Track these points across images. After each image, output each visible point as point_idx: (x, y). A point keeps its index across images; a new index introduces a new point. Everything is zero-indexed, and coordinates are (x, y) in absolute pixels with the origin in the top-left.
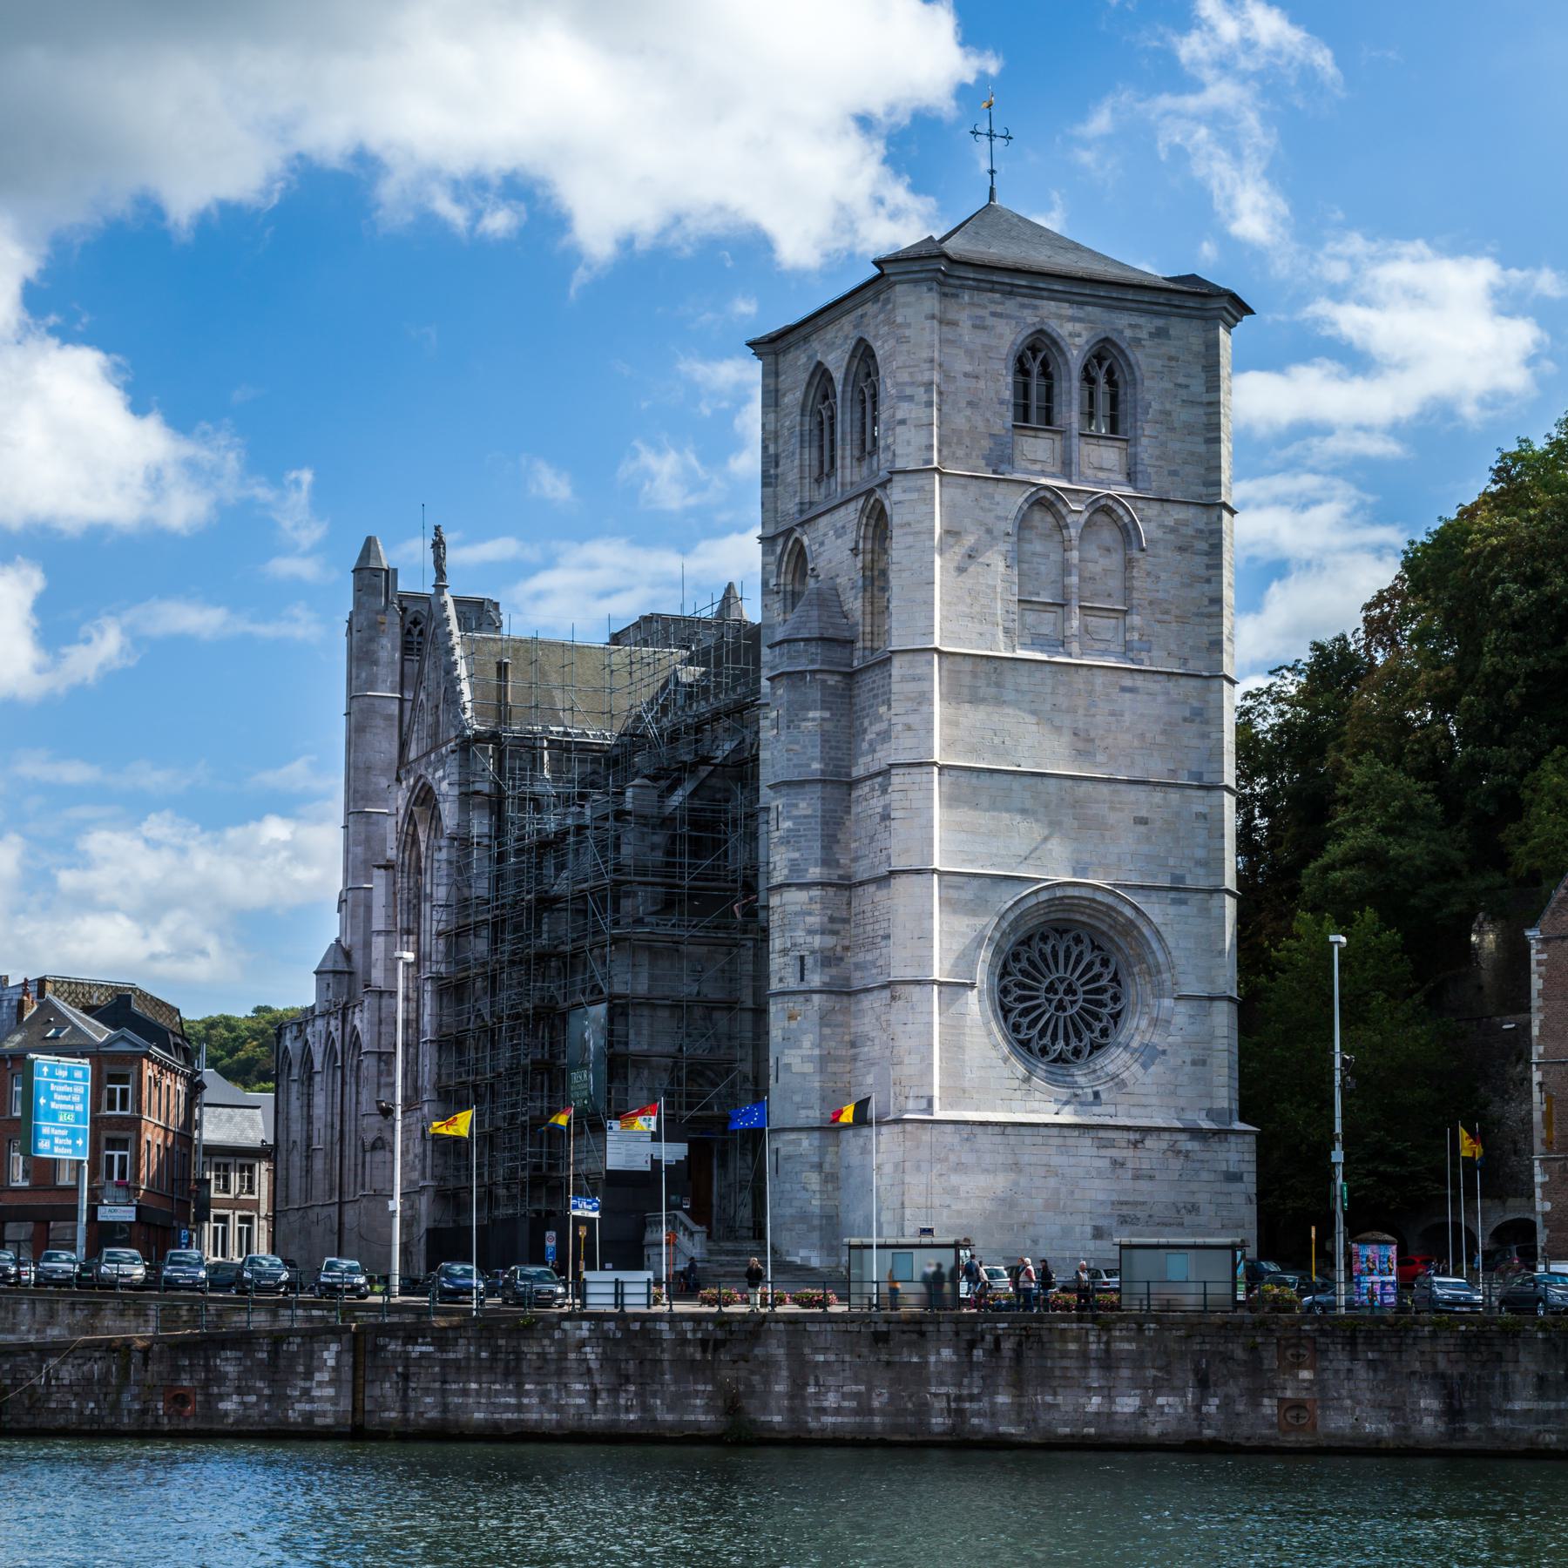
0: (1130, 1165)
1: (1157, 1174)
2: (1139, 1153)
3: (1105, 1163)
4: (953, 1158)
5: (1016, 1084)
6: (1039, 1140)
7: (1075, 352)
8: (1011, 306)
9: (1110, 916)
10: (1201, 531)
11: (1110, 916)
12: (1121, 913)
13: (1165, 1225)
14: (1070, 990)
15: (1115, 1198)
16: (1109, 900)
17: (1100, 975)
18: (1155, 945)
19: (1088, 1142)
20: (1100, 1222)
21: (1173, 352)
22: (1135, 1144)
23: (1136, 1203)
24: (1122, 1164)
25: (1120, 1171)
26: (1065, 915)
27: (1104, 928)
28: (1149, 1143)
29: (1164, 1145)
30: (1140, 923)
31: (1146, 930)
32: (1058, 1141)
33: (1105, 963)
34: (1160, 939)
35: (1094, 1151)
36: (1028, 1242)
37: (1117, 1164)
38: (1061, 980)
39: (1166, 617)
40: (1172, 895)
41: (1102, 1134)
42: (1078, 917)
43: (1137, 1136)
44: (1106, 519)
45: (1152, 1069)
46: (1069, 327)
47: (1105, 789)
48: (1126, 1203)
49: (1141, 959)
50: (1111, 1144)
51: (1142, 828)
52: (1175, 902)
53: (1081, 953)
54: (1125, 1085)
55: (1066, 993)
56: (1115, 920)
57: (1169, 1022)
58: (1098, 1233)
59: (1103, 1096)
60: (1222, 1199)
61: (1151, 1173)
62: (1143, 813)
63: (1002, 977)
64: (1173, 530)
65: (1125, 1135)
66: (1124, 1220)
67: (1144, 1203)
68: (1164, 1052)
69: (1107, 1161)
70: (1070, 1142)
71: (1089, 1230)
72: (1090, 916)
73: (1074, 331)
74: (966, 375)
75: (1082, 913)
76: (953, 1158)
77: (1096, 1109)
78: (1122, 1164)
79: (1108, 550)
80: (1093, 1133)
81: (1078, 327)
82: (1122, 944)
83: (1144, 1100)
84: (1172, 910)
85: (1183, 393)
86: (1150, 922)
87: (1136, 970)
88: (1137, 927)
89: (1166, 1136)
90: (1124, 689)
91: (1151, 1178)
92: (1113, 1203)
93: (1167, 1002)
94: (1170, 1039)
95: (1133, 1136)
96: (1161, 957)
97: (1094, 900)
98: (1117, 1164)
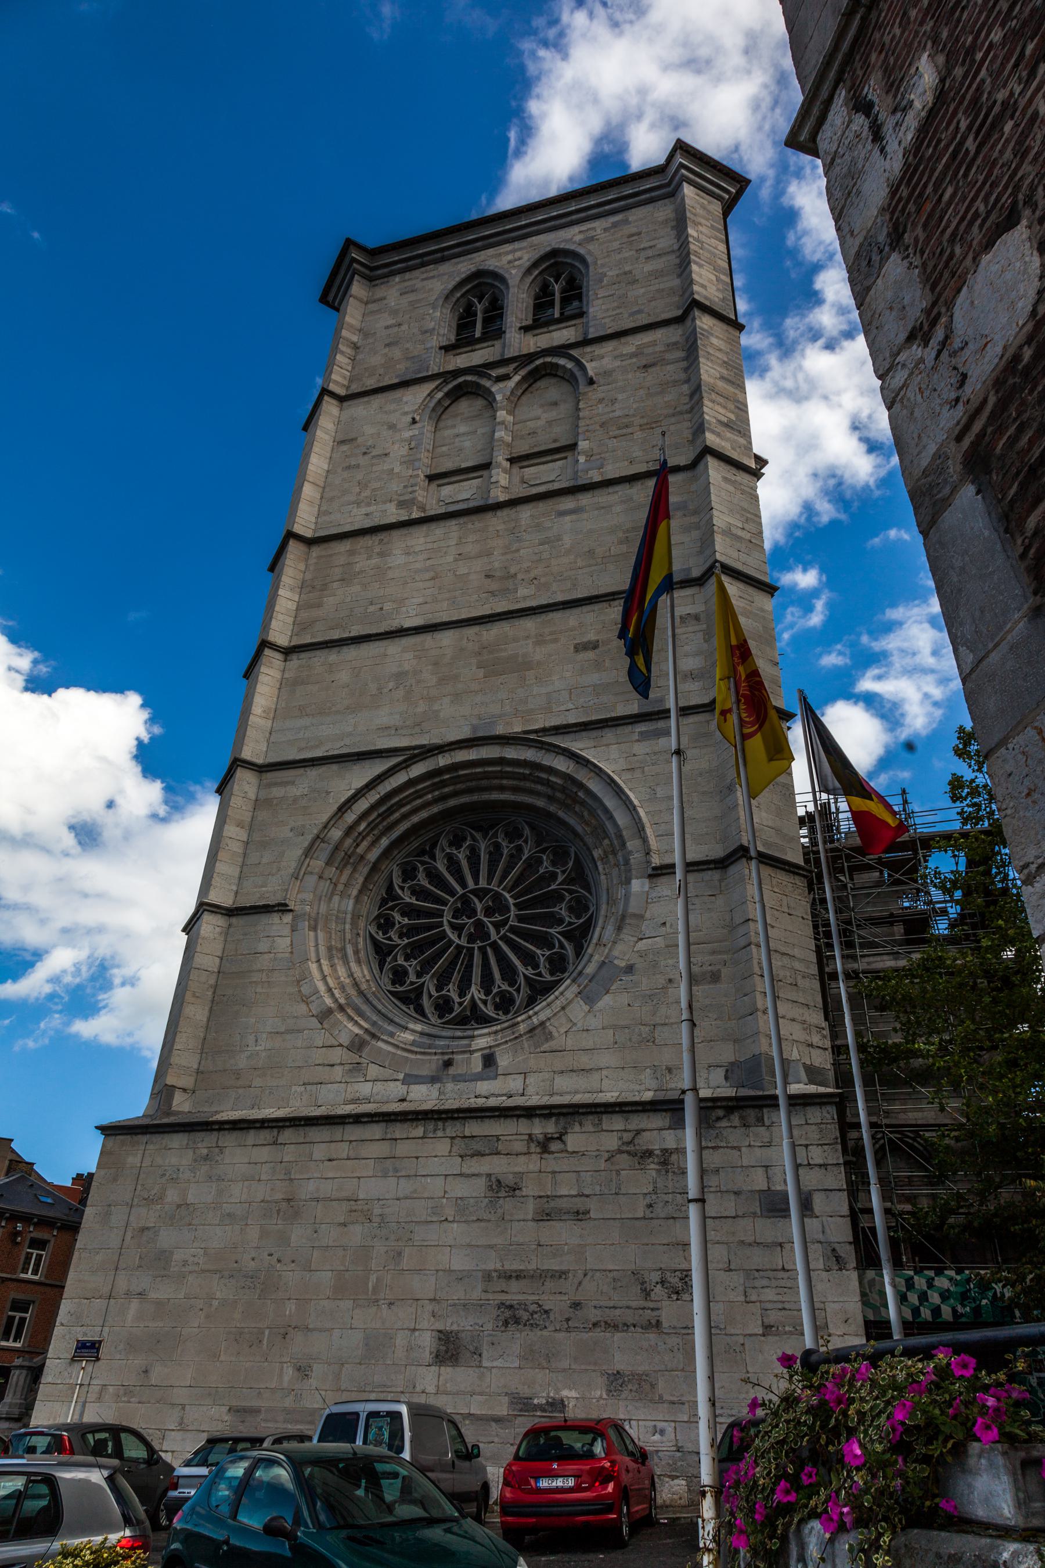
0: (530, 1189)
1: (592, 1205)
2: (552, 1163)
3: (475, 1189)
4: (172, 1196)
5: (337, 1055)
6: (343, 1150)
7: (513, 272)
8: (445, 268)
9: (540, 781)
10: (675, 343)
11: (540, 781)
12: (551, 770)
13: (613, 1326)
14: (498, 906)
15: (492, 1264)
16: (529, 754)
17: (553, 876)
18: (610, 802)
19: (442, 1147)
20: (449, 1324)
21: (634, 230)
22: (544, 1145)
23: (542, 1276)
24: (514, 1189)
25: (507, 1205)
26: (475, 797)
27: (540, 803)
28: (574, 1140)
29: (611, 1142)
30: (582, 775)
31: (594, 785)
32: (381, 1149)
33: (560, 855)
34: (618, 792)
35: (455, 1165)
36: (289, 1372)
37: (503, 1189)
38: (480, 893)
39: (629, 430)
40: (642, 727)
41: (473, 1128)
42: (495, 796)
43: (550, 1127)
44: (553, 380)
45: (606, 1001)
46: (510, 257)
47: (529, 624)
48: (519, 1276)
49: (600, 832)
50: (493, 1148)
51: (590, 655)
52: (644, 736)
53: (519, 849)
54: (549, 1037)
55: (489, 912)
56: (548, 783)
57: (641, 917)
58: (450, 1350)
59: (503, 1061)
60: (757, 1258)
61: (579, 1204)
62: (592, 636)
63: (384, 902)
64: (633, 355)
65: (523, 1127)
66: (512, 1317)
67: (562, 1274)
68: (630, 969)
69: (482, 1182)
70: (403, 1149)
71: (427, 1341)
72: (515, 790)
73: (513, 261)
74: (387, 327)
75: (502, 789)
76: (172, 1196)
77: (484, 1087)
78: (514, 1189)
79: (556, 404)
80: (452, 1129)
81: (518, 254)
82: (572, 821)
83: (585, 1061)
84: (641, 749)
85: (650, 253)
86: (598, 771)
87: (597, 853)
88: (581, 786)
89: (617, 1123)
90: (562, 514)
91: (580, 1215)
92: (488, 1276)
93: (637, 885)
94: (641, 945)
95: (539, 1128)
96: (621, 818)
97: (502, 761)
98: (503, 1189)
